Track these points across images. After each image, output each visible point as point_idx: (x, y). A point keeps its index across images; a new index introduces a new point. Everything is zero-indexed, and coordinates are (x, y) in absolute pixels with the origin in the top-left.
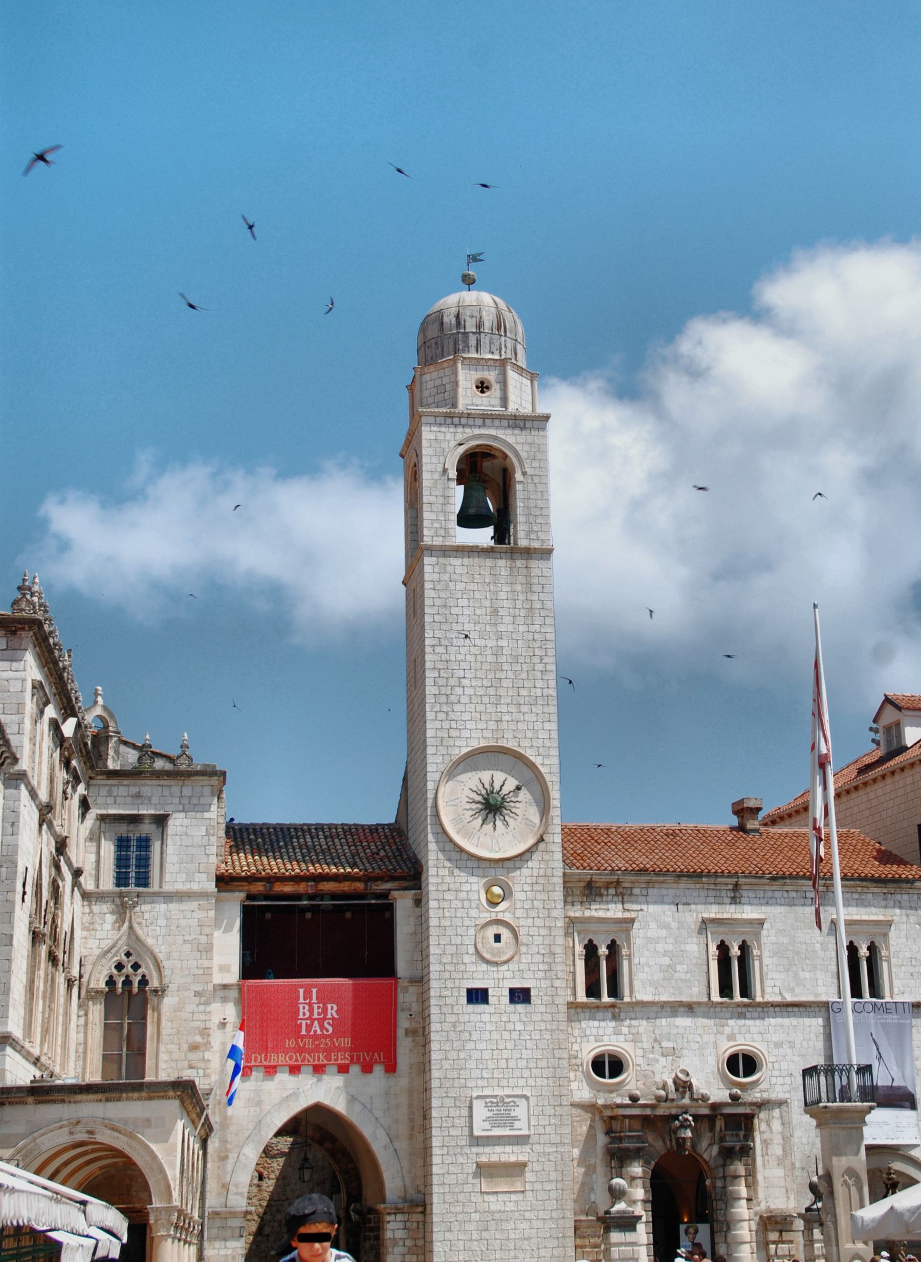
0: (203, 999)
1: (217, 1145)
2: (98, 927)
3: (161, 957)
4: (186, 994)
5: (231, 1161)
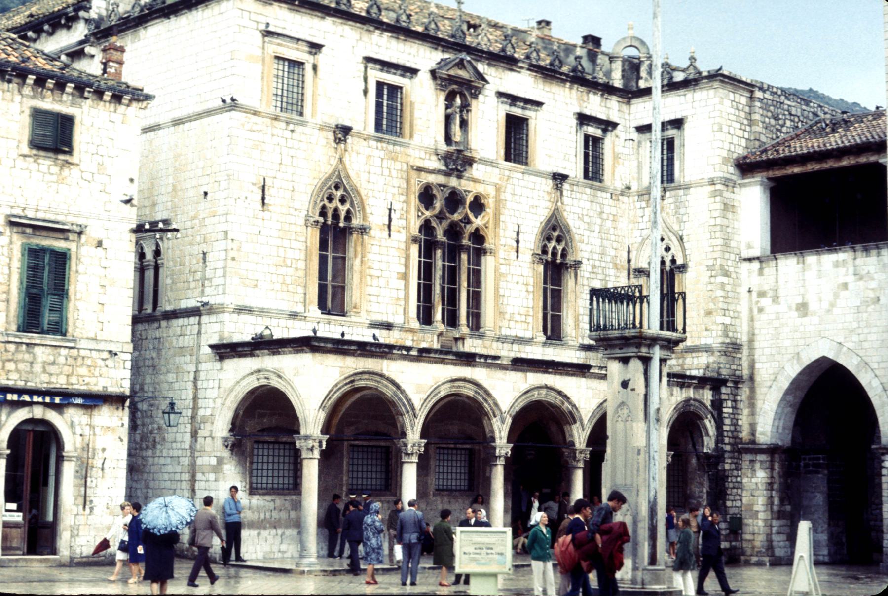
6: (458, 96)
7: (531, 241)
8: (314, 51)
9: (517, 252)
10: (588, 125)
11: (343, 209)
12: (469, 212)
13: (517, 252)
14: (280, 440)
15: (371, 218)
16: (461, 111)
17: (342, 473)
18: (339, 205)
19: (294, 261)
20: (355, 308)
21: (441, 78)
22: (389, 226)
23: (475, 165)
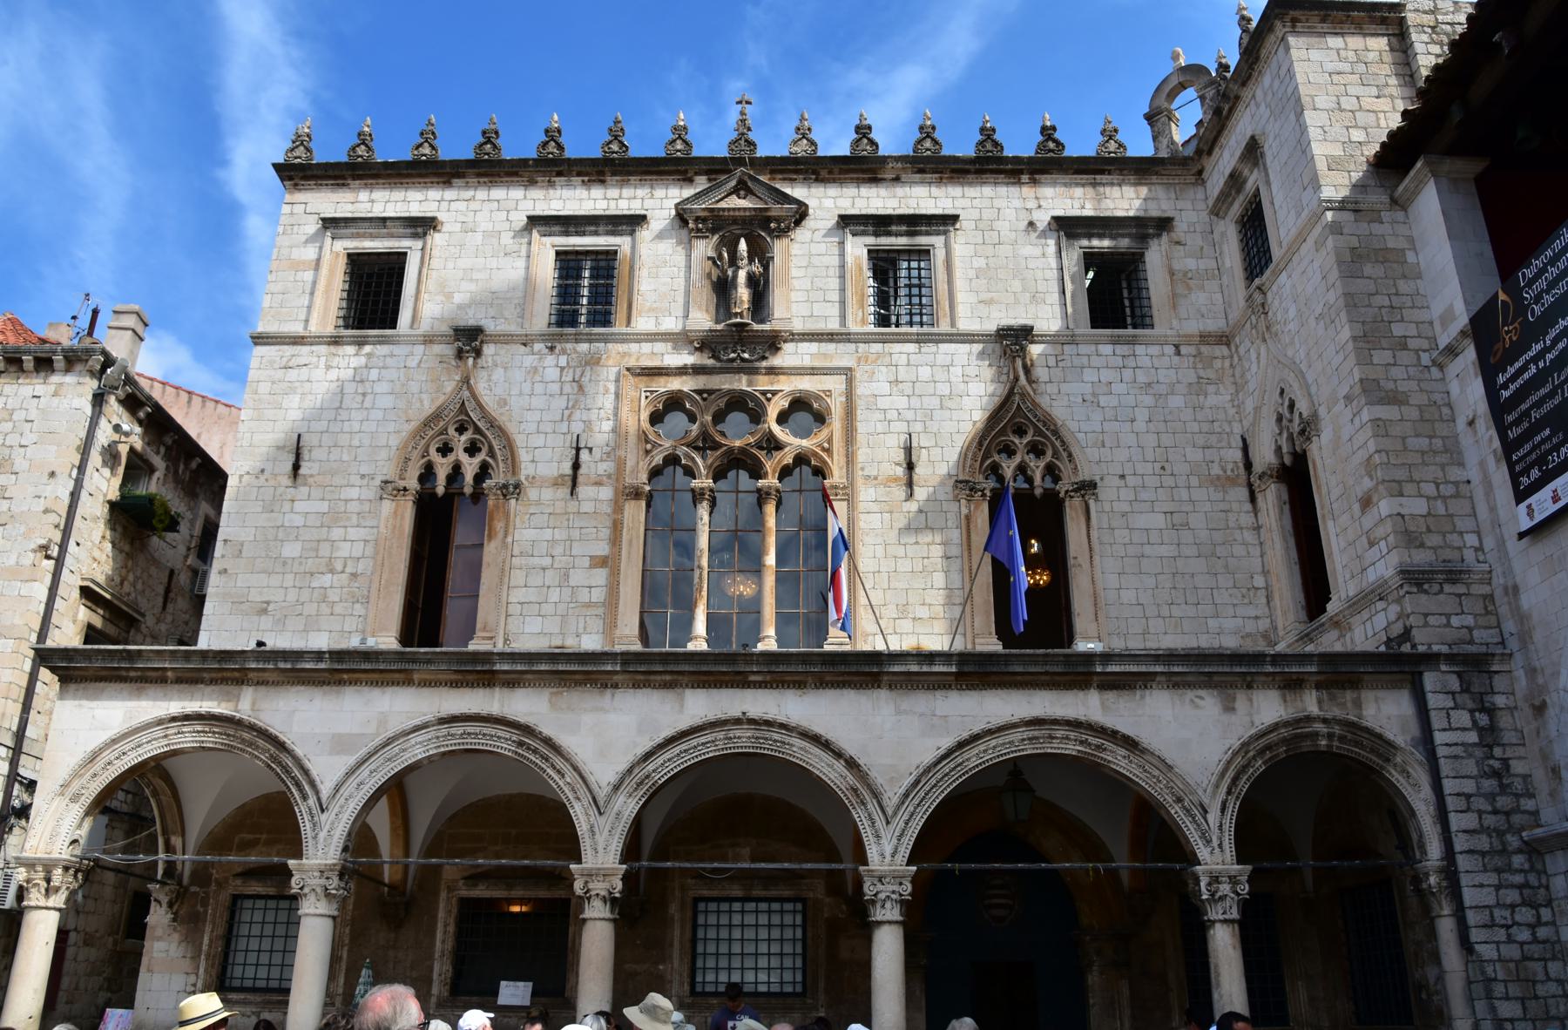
1: (1524, 683)
3: (1303, 367)
5: (1551, 712)
6: (743, 241)
8: (420, 230)
11: (470, 467)
13: (910, 484)
15: (526, 470)
17: (431, 957)
18: (464, 458)
20: (484, 629)
21: (697, 219)
23: (788, 347)
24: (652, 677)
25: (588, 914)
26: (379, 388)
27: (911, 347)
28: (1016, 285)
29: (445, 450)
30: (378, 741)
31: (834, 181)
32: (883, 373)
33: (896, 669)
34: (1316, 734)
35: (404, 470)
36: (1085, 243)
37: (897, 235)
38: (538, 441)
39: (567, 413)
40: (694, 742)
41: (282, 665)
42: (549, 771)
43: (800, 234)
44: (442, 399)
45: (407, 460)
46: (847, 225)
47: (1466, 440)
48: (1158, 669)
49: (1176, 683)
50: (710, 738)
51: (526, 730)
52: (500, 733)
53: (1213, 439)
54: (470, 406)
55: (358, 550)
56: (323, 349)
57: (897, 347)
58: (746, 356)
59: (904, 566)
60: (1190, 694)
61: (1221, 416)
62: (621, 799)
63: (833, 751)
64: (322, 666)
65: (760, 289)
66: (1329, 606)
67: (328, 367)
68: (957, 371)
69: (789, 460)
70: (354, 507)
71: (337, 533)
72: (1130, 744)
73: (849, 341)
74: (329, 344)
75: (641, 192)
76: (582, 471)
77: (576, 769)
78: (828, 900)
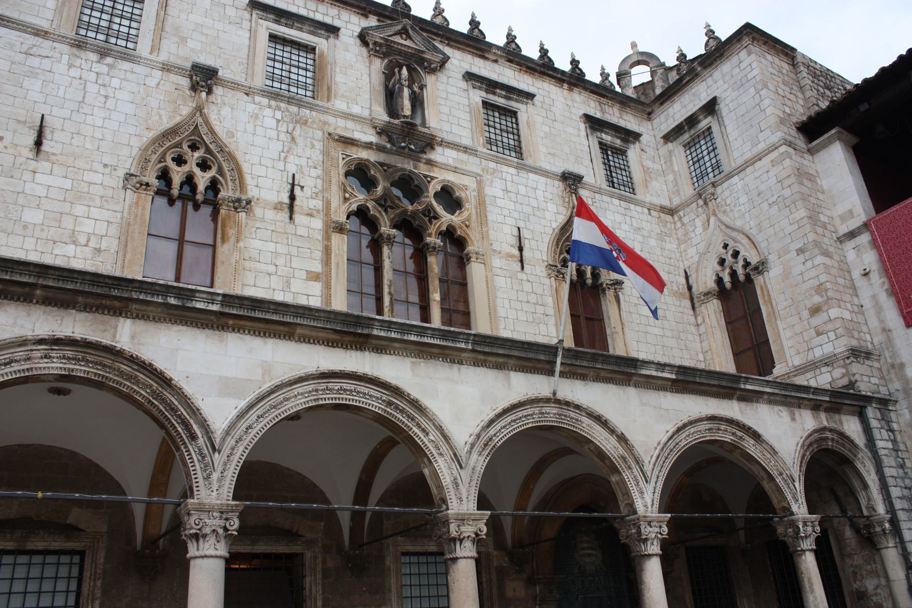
0: (807, 254)
2: (692, 235)
3: (753, 232)
4: (788, 257)
6: (404, 68)
7: (540, 250)
9: (522, 261)
10: (601, 131)
11: (202, 180)
12: (435, 204)
13: (522, 261)
14: (30, 546)
16: (409, 87)
18: (197, 171)
19: (92, 238)
21: (375, 43)
22: (291, 207)
23: (439, 149)
24: (490, 358)
25: (459, 552)
26: (120, 95)
27: (513, 171)
28: (567, 149)
29: (180, 161)
30: (266, 387)
31: (459, 49)
32: (498, 183)
33: (644, 372)
34: (826, 439)
35: (144, 169)
36: (599, 134)
37: (500, 96)
38: (261, 171)
39: (283, 155)
40: (520, 414)
41: (172, 301)
42: (414, 429)
43: (442, 77)
44: (178, 119)
45: (147, 161)
46: (471, 79)
47: (861, 283)
48: (768, 390)
49: (770, 402)
50: (530, 411)
51: (397, 391)
52: (372, 392)
53: (672, 268)
54: (203, 130)
55: (101, 228)
56: (66, 48)
57: (505, 168)
58: (412, 147)
59: (522, 316)
60: (777, 408)
61: (674, 257)
62: (474, 456)
63: (609, 428)
64: (215, 308)
65: (417, 102)
66: (775, 371)
67: (71, 66)
68: (540, 193)
69: (444, 228)
70: (97, 190)
71: (79, 210)
72: (756, 436)
73: (476, 155)
74: (72, 45)
75: (334, 11)
76: (297, 202)
77: (440, 429)
78: (496, 553)
